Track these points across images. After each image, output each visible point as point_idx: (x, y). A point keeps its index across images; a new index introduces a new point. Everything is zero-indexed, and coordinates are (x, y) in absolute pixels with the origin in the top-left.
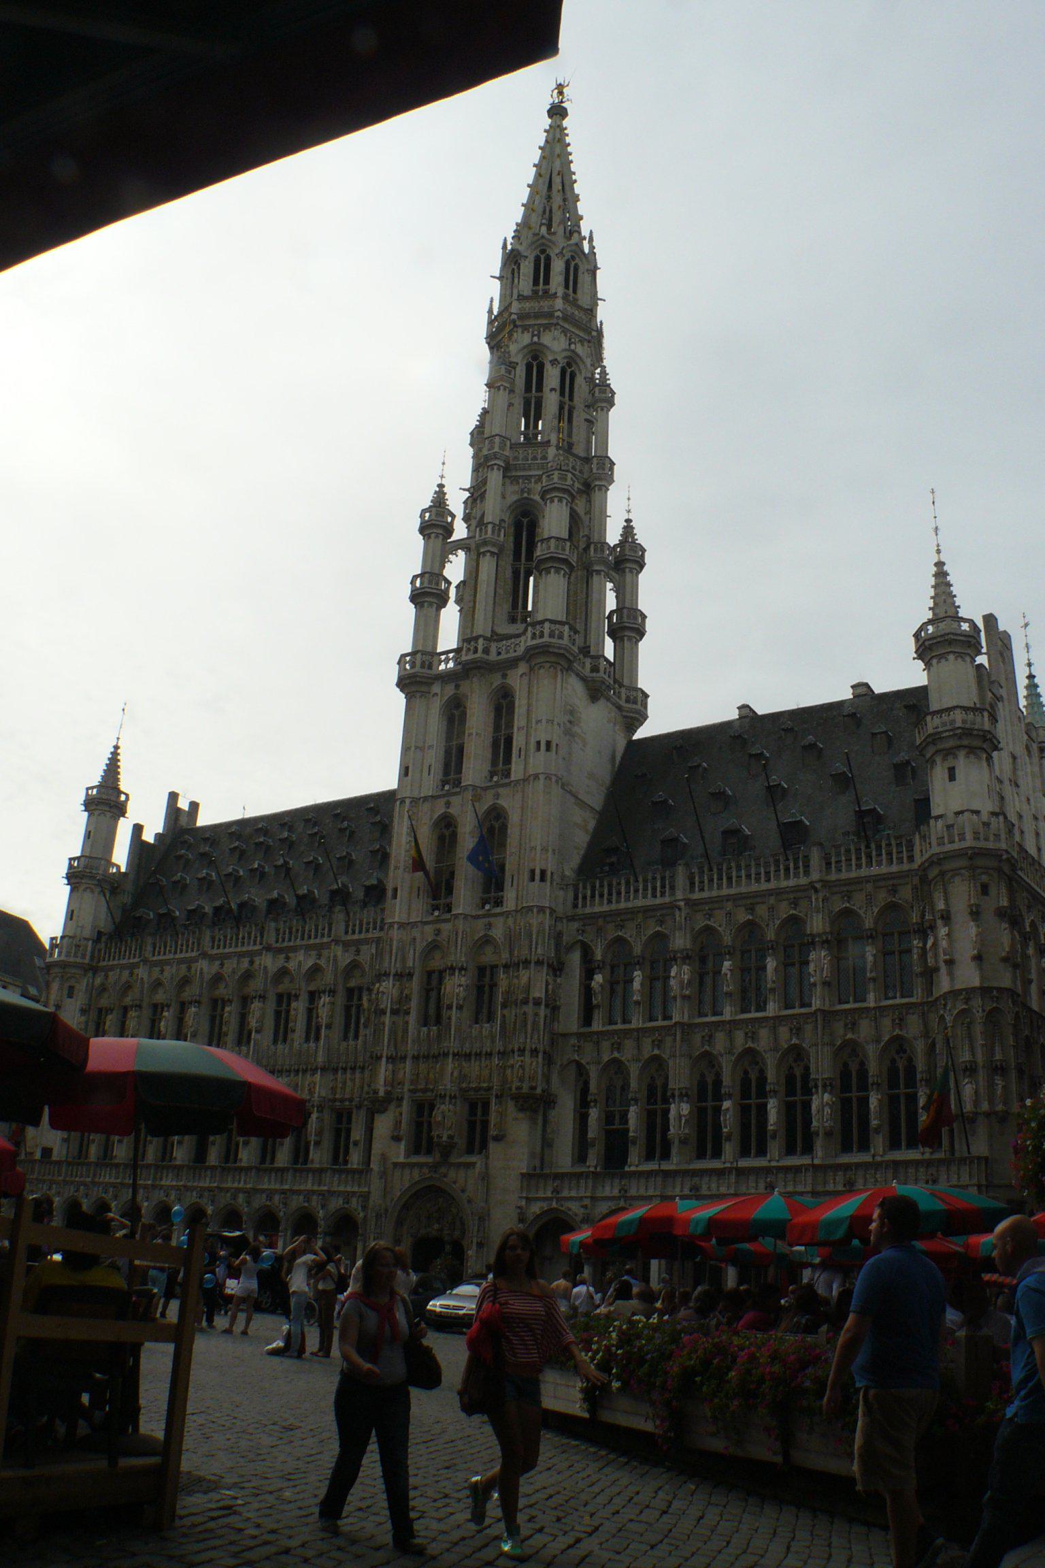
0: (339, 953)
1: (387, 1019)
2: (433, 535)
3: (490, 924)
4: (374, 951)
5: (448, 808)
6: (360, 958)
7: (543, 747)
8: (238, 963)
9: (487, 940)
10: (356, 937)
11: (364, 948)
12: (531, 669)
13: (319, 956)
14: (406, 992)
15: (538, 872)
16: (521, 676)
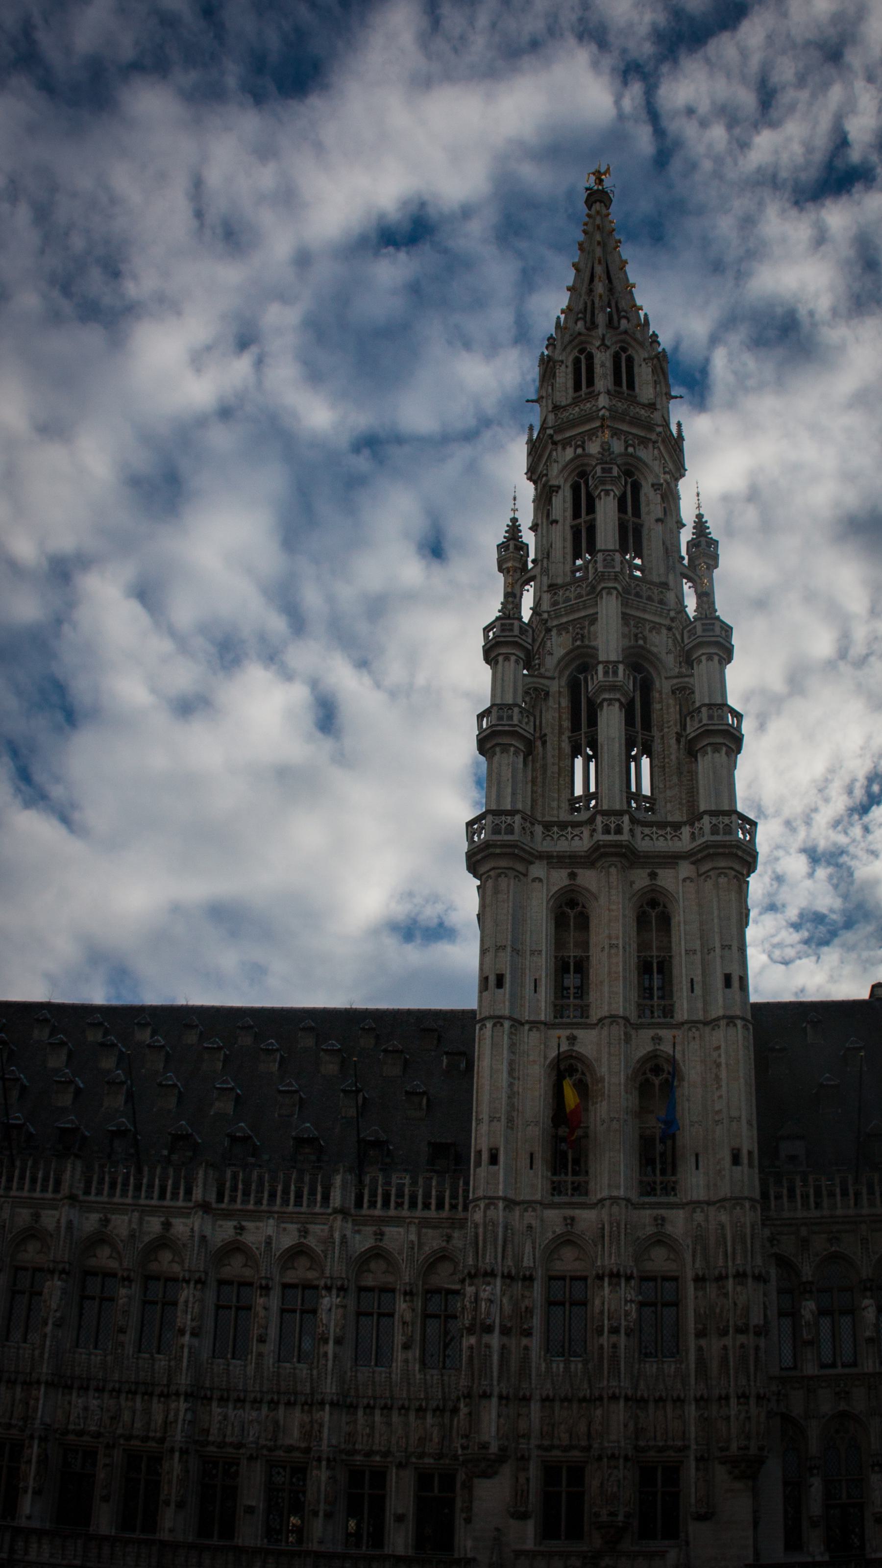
0: (349, 1233)
1: (495, 1340)
2: (501, 659)
3: (663, 1219)
4: (413, 1237)
5: (573, 1044)
6: (387, 1244)
7: (736, 983)
8: (141, 1222)
9: (661, 1240)
10: (378, 1212)
11: (391, 1231)
12: (699, 875)
13: (304, 1233)
14: (527, 1302)
15: (745, 1152)
16: (684, 880)
